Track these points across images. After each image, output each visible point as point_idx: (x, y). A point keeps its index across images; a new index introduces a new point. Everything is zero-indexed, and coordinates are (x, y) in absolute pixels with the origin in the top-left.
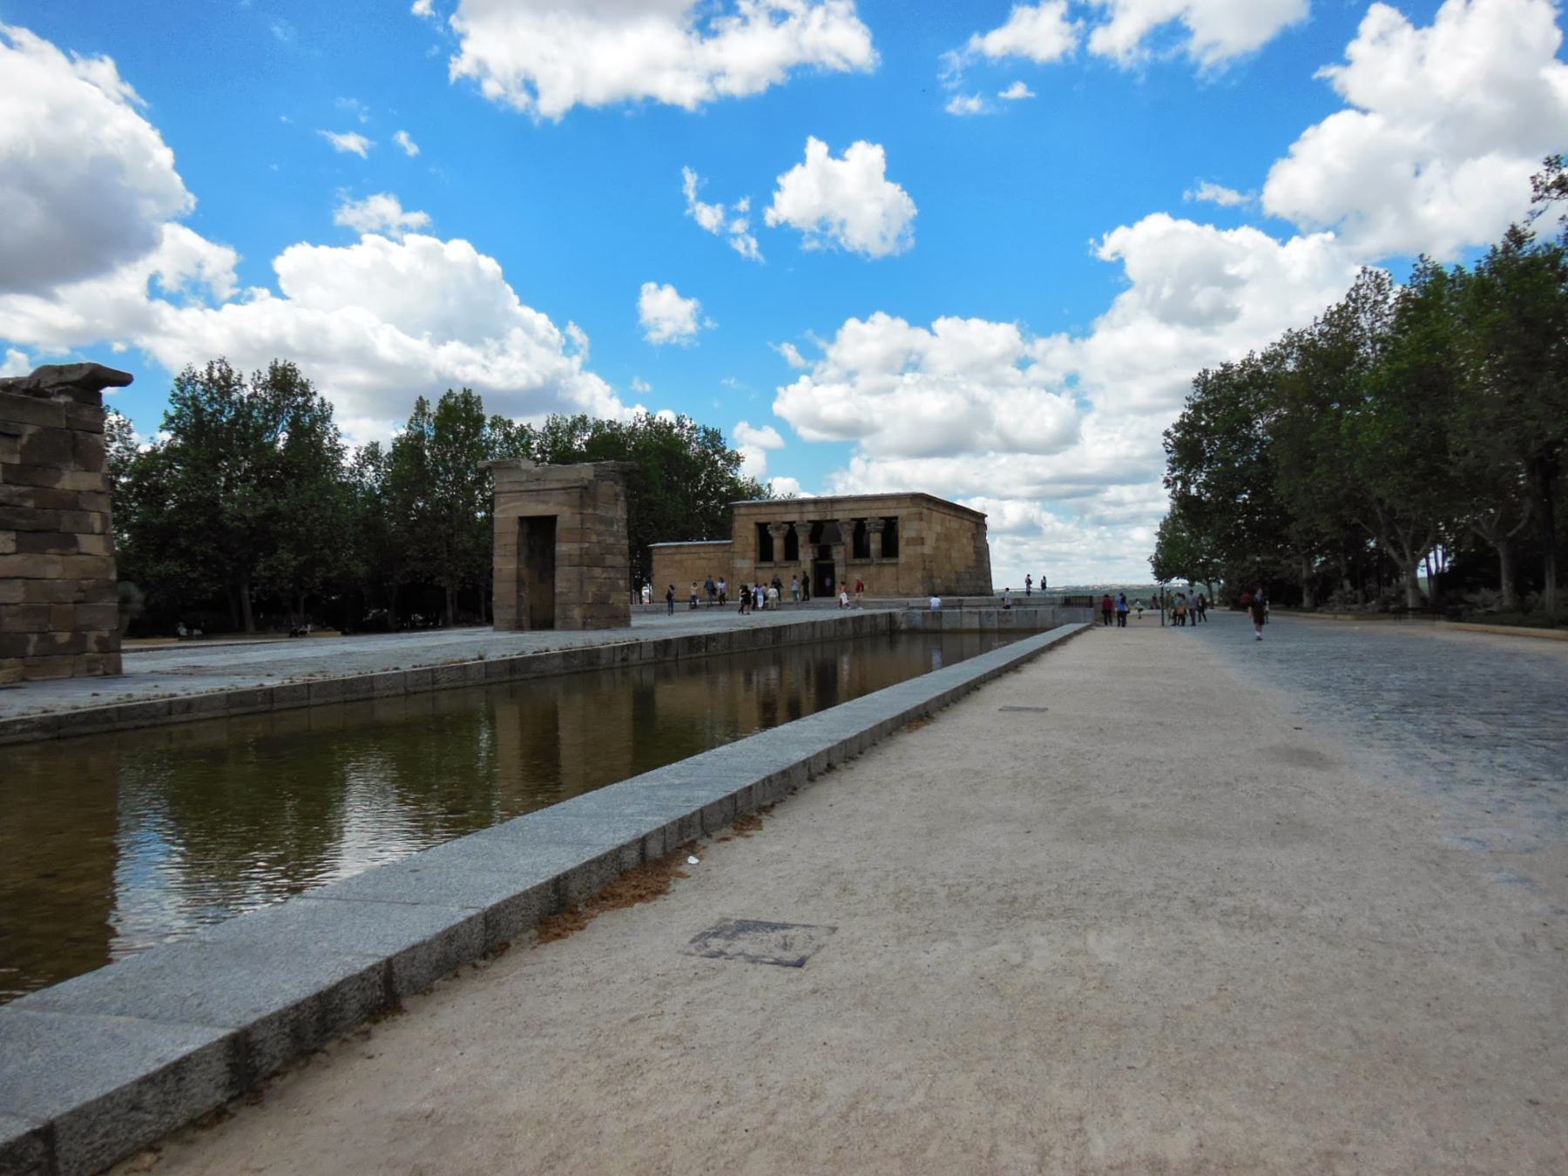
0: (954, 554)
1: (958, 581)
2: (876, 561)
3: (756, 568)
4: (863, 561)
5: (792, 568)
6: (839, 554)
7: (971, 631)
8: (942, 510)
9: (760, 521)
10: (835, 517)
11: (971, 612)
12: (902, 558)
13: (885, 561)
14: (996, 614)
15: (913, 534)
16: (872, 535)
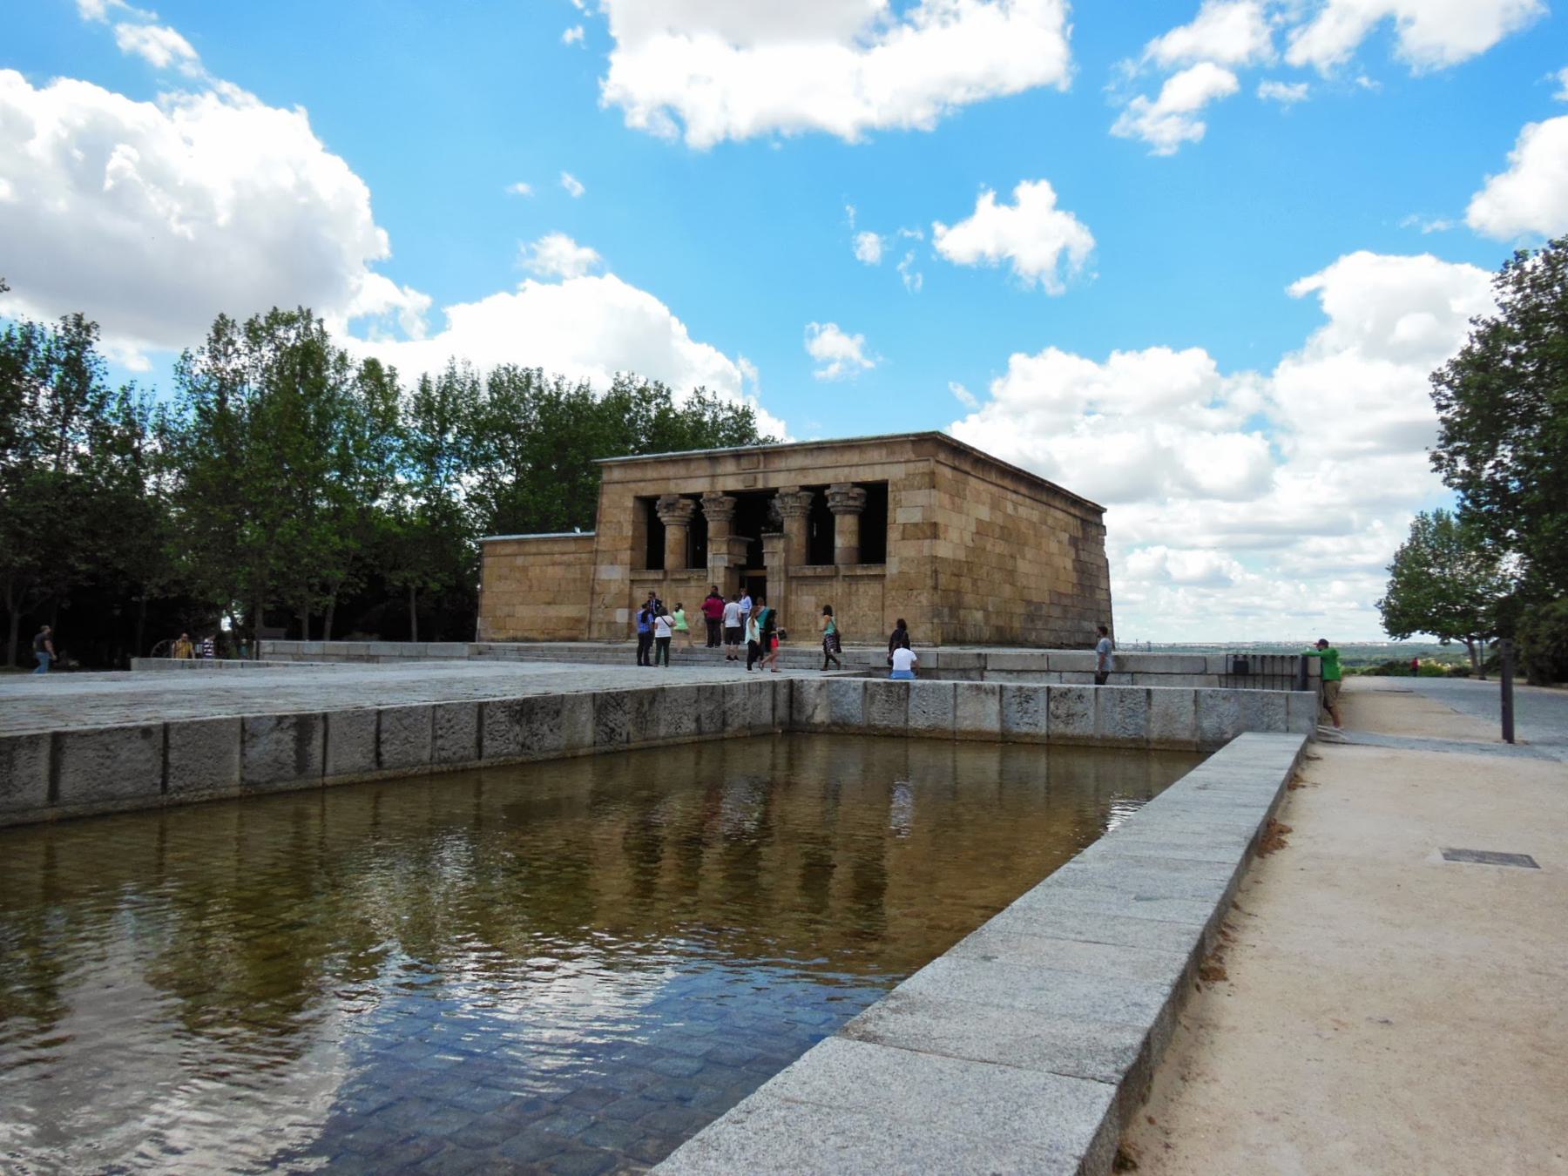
0: (1023, 566)
1: (1031, 618)
2: (843, 571)
3: (632, 581)
4: (819, 570)
5: (693, 583)
6: (775, 555)
7: (980, 740)
8: (993, 477)
9: (644, 494)
10: (772, 484)
11: (978, 688)
12: (892, 566)
13: (859, 572)
14: (1042, 696)
15: (917, 517)
16: (838, 519)
